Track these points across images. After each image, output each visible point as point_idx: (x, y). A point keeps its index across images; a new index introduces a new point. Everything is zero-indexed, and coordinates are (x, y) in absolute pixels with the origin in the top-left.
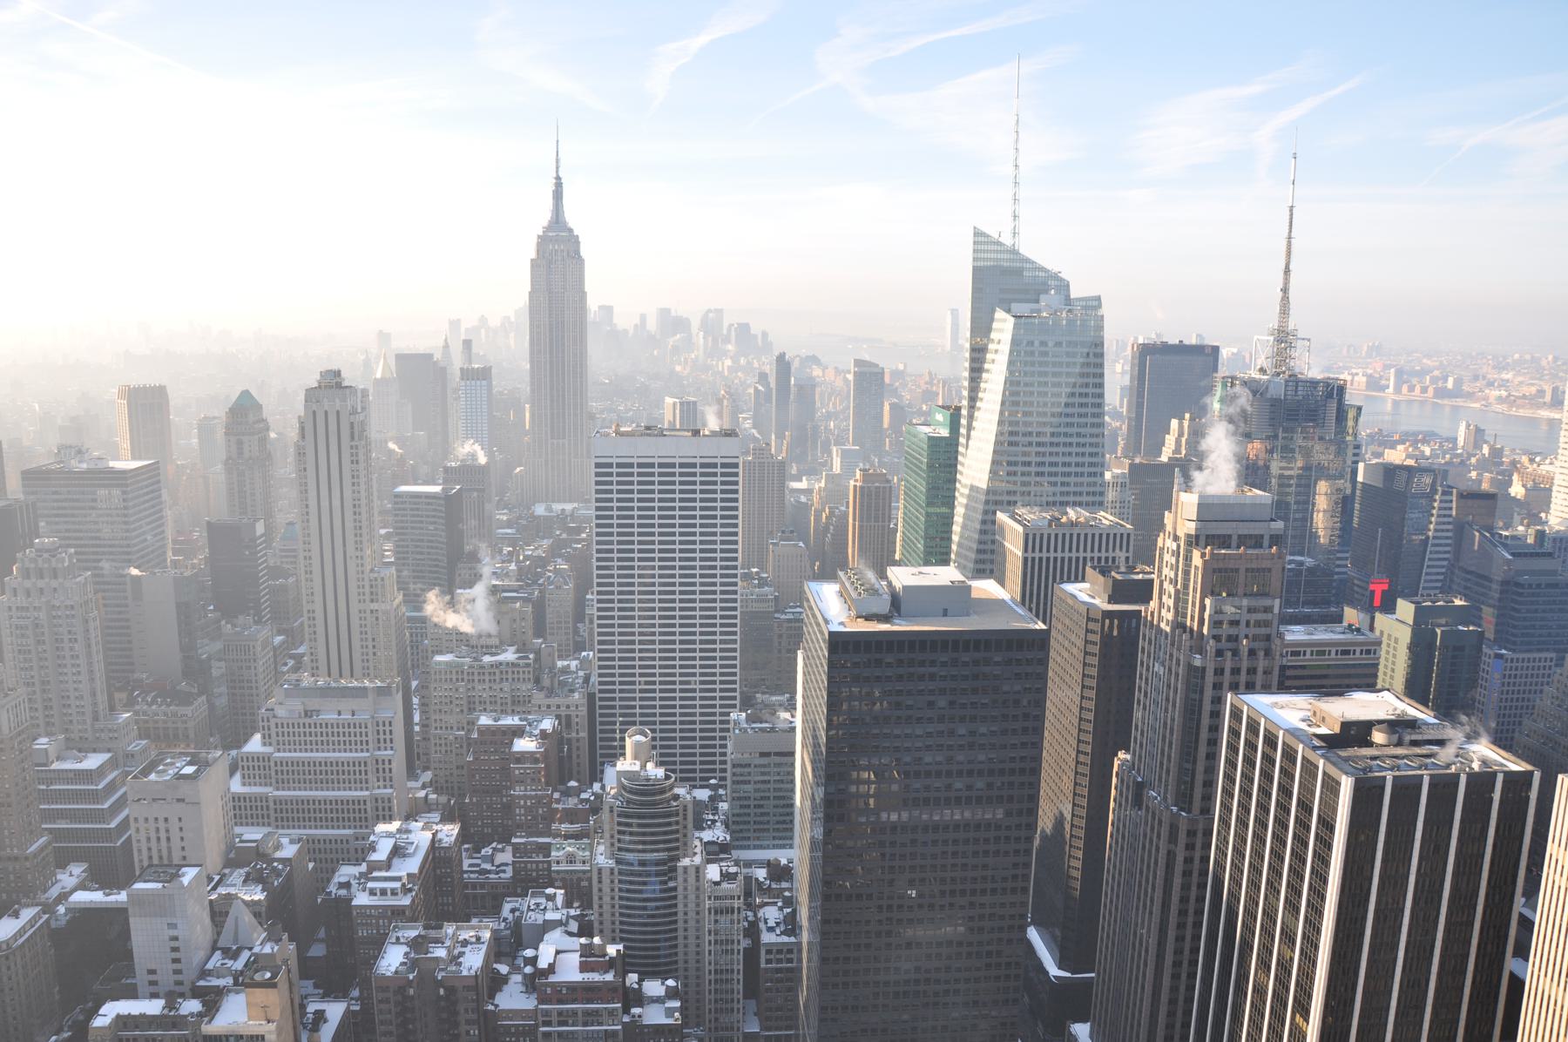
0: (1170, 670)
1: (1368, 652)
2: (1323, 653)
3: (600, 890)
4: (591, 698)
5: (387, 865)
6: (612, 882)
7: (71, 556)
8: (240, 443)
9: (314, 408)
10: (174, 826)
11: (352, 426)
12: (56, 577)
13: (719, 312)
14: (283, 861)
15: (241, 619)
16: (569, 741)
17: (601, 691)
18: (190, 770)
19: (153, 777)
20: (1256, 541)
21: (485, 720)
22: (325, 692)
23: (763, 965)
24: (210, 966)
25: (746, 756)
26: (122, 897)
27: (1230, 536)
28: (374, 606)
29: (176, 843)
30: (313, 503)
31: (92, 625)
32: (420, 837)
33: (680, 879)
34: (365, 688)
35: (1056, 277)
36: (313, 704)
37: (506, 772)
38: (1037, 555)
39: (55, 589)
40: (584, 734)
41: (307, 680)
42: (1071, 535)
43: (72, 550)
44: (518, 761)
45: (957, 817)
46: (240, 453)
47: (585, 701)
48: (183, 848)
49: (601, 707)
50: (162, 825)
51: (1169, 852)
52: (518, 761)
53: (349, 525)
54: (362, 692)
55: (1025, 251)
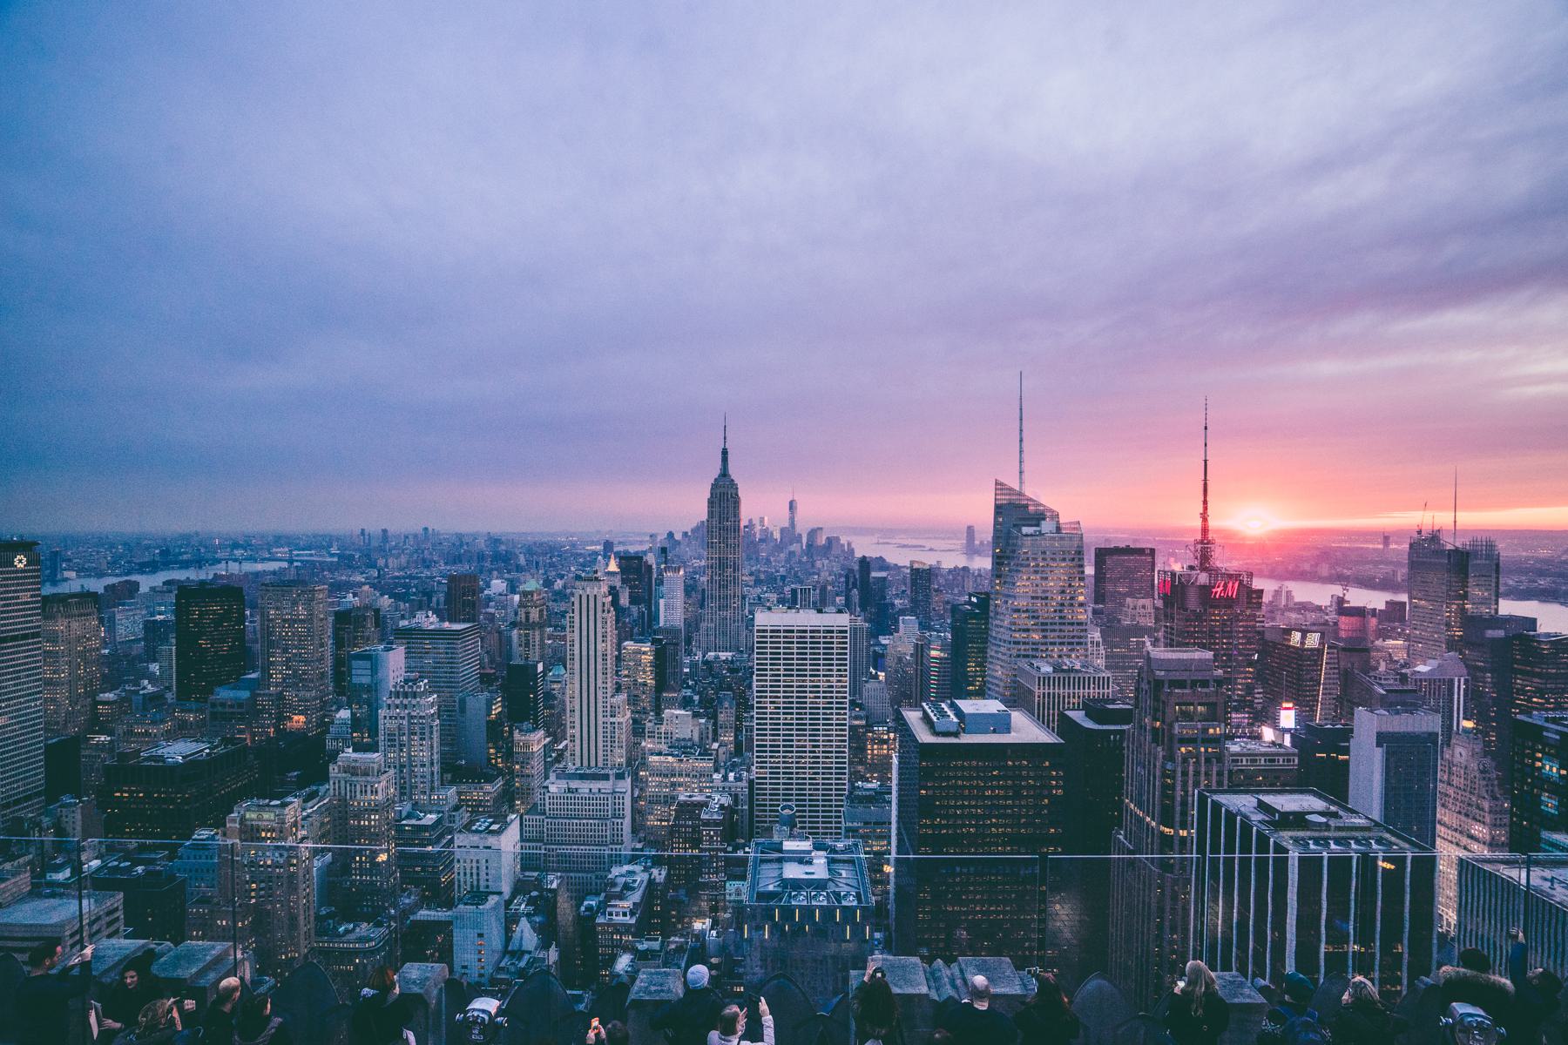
0: (1149, 771)
1: (1289, 761)
4: (751, 782)
5: (621, 897)
7: (425, 685)
8: (527, 614)
12: (415, 697)
13: (821, 529)
14: (551, 891)
16: (736, 812)
17: (758, 778)
18: (494, 827)
20: (1205, 684)
21: (682, 798)
24: (502, 964)
25: (855, 824)
27: (1185, 681)
28: (612, 720)
30: (577, 652)
31: (435, 729)
32: (641, 877)
34: (608, 775)
35: (1051, 511)
36: (574, 784)
39: (414, 706)
40: (746, 807)
41: (571, 769)
42: (1069, 678)
43: (426, 681)
47: (747, 785)
48: (487, 880)
49: (757, 789)
55: (1029, 492)
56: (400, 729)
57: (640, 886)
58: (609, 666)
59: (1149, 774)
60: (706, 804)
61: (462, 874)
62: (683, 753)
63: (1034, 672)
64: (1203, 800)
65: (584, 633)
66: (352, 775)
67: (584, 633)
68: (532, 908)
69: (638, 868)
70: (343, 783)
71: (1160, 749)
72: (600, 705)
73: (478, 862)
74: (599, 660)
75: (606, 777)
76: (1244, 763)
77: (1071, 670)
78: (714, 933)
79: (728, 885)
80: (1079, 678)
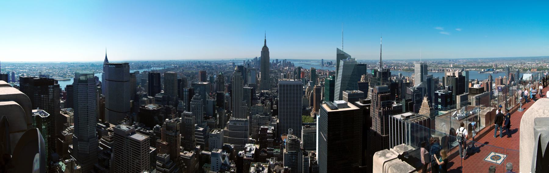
8: (220, 80)
9: (235, 75)
10: (216, 141)
11: (241, 78)
13: (286, 60)
15: (221, 108)
18: (218, 132)
19: (213, 133)
21: (262, 127)
22: (238, 121)
26: (210, 153)
28: (243, 107)
29: (216, 145)
30: (234, 90)
31: (202, 108)
33: (298, 156)
36: (235, 122)
37: (265, 135)
41: (234, 119)
46: (220, 81)
53: (240, 93)
57: (254, 149)
58: (242, 93)
60: (267, 129)
65: (236, 85)
67: (236, 85)
69: (253, 145)
72: (240, 103)
73: (215, 140)
74: (240, 91)
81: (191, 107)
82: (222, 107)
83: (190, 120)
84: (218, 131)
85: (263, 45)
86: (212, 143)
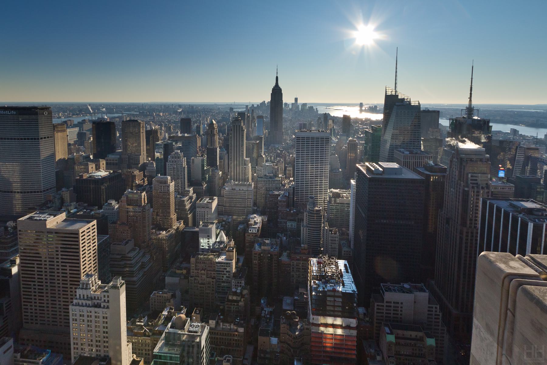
2: (496, 188)
3: (303, 233)
6: (306, 231)
8: (211, 131)
14: (228, 222)
17: (296, 187)
18: (211, 201)
23: (343, 255)
28: (245, 166)
38: (407, 160)
42: (416, 156)
44: (280, 202)
45: (401, 222)
46: (212, 133)
50: (203, 213)
51: (460, 237)
52: (280, 202)
54: (245, 185)
56: (174, 168)
59: (457, 191)
60: (279, 195)
61: (199, 216)
62: (270, 178)
63: (402, 154)
64: (484, 203)
66: (161, 183)
68: (223, 228)
70: (157, 186)
71: (462, 183)
73: (204, 212)
75: (245, 185)
76: (507, 189)
77: (417, 153)
78: (285, 238)
79: (288, 222)
80: (420, 156)
81: (167, 170)
82: (214, 167)
83: (166, 187)
84: (209, 199)
85: (274, 84)
86: (200, 216)
